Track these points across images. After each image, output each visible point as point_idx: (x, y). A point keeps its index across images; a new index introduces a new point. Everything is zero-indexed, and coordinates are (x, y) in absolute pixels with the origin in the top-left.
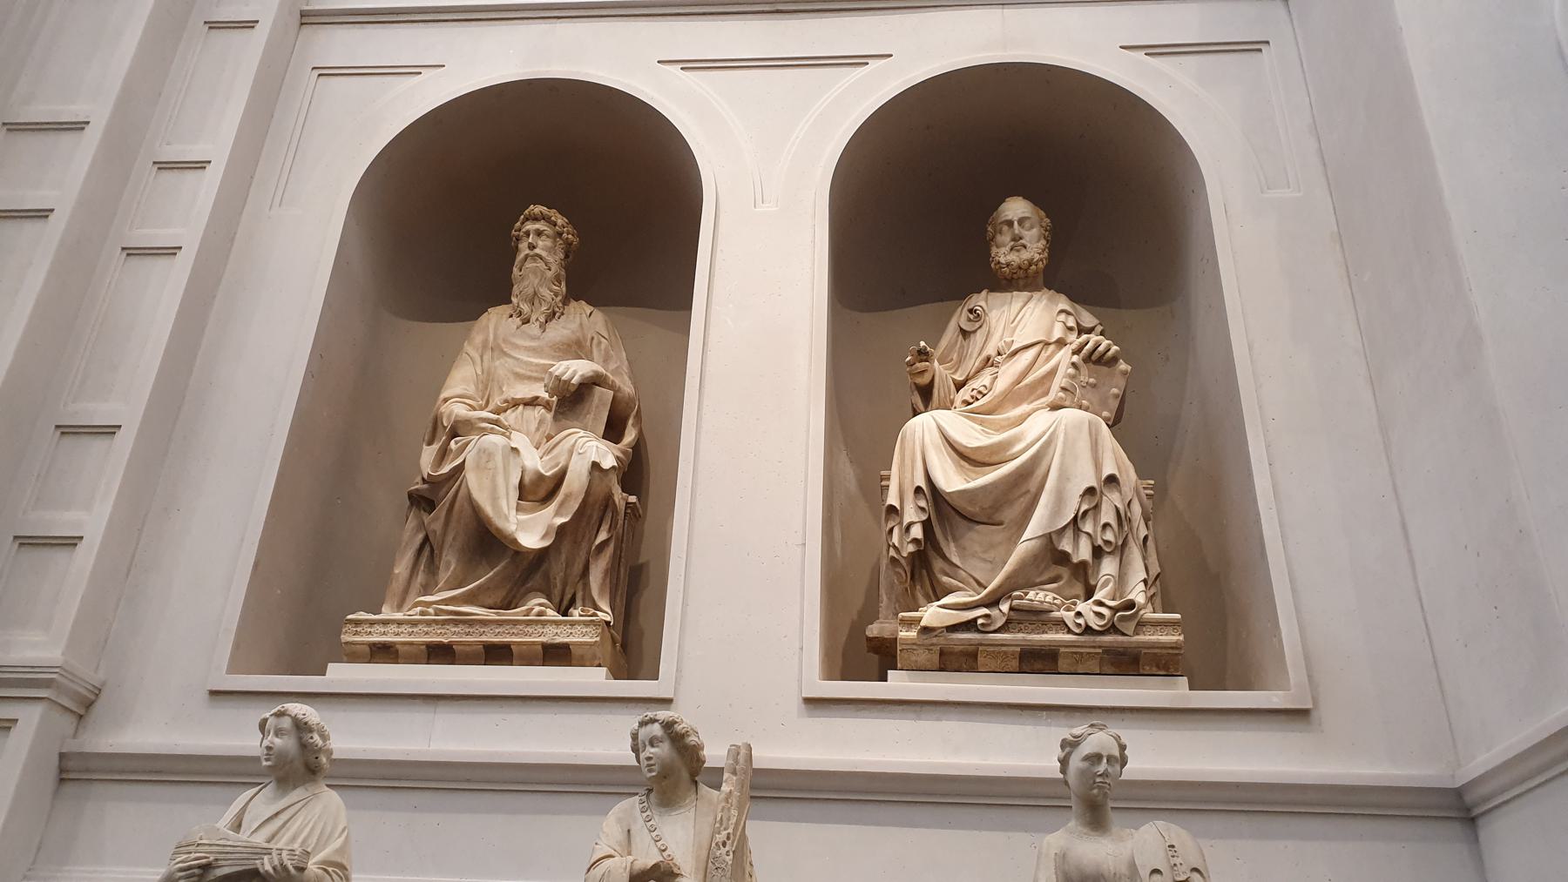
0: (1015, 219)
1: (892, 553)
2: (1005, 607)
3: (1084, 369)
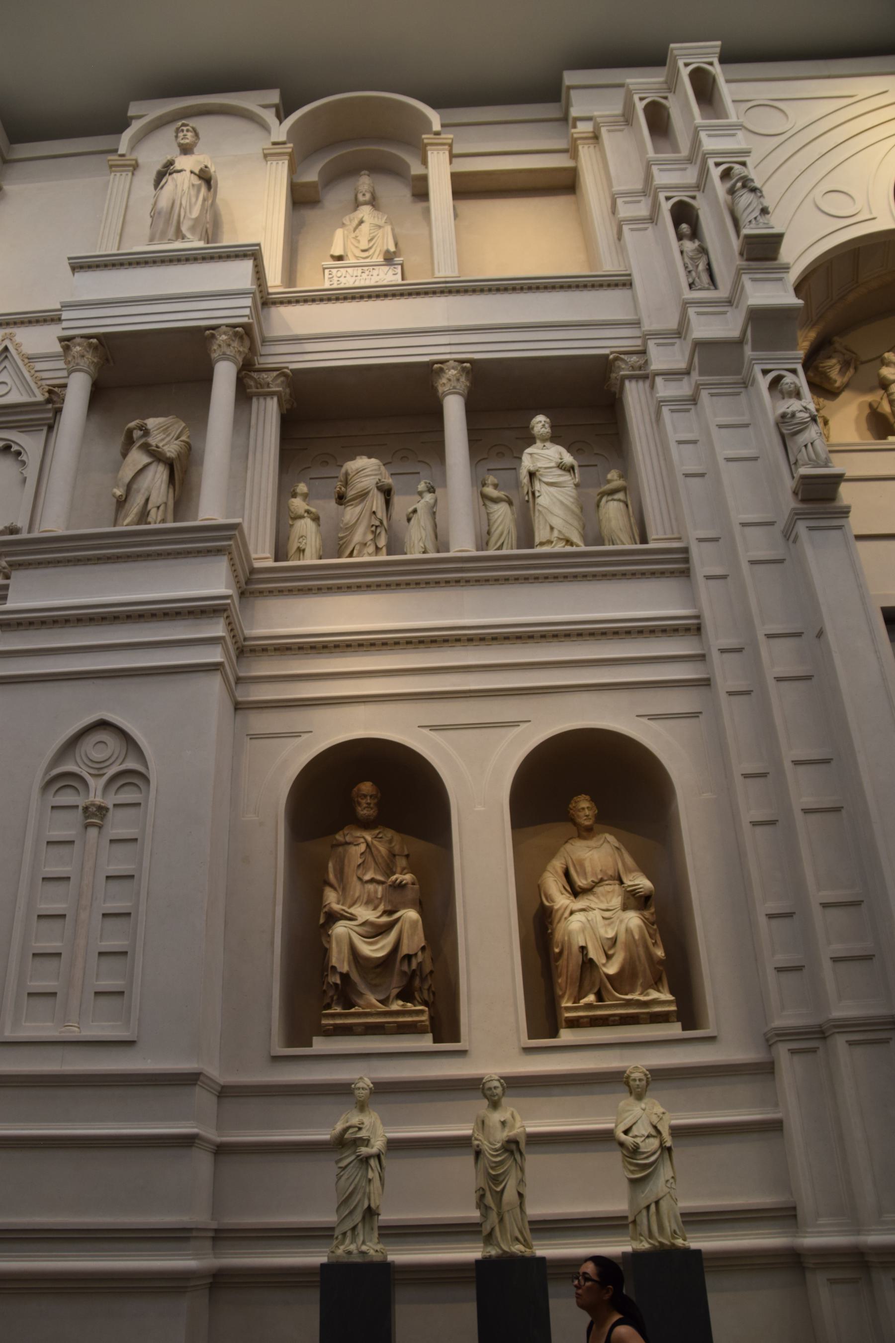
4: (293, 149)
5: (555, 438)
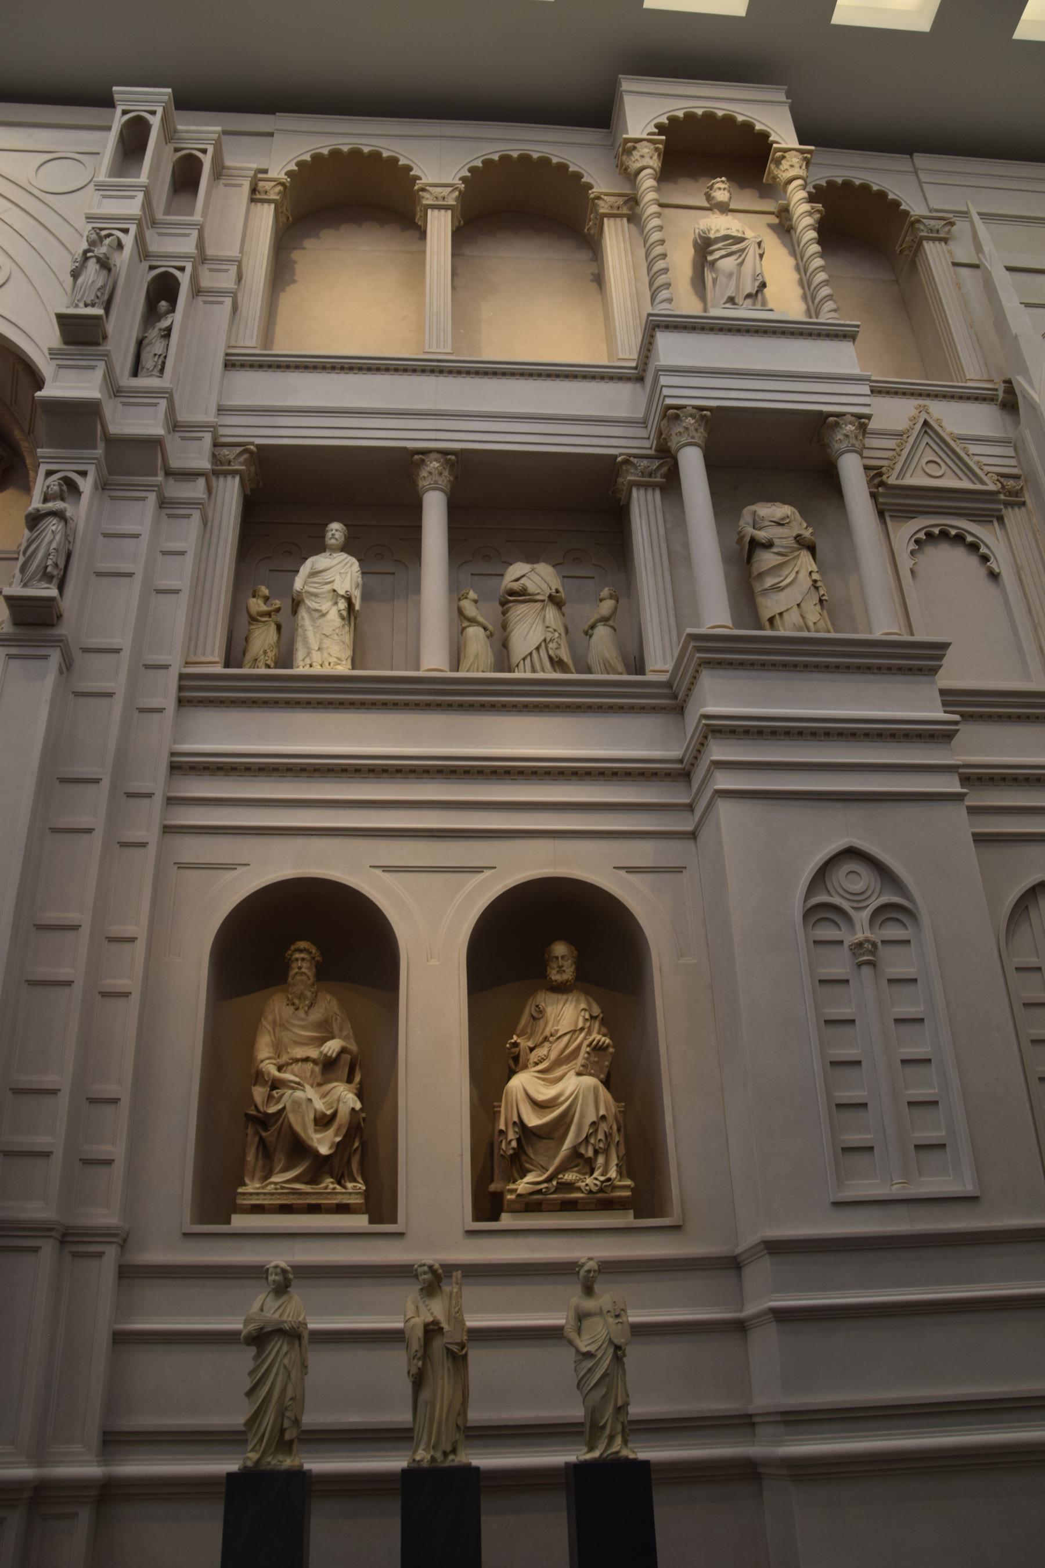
0: (560, 956)
1: (502, 1152)
2: (554, 1183)
3: (593, 1055)
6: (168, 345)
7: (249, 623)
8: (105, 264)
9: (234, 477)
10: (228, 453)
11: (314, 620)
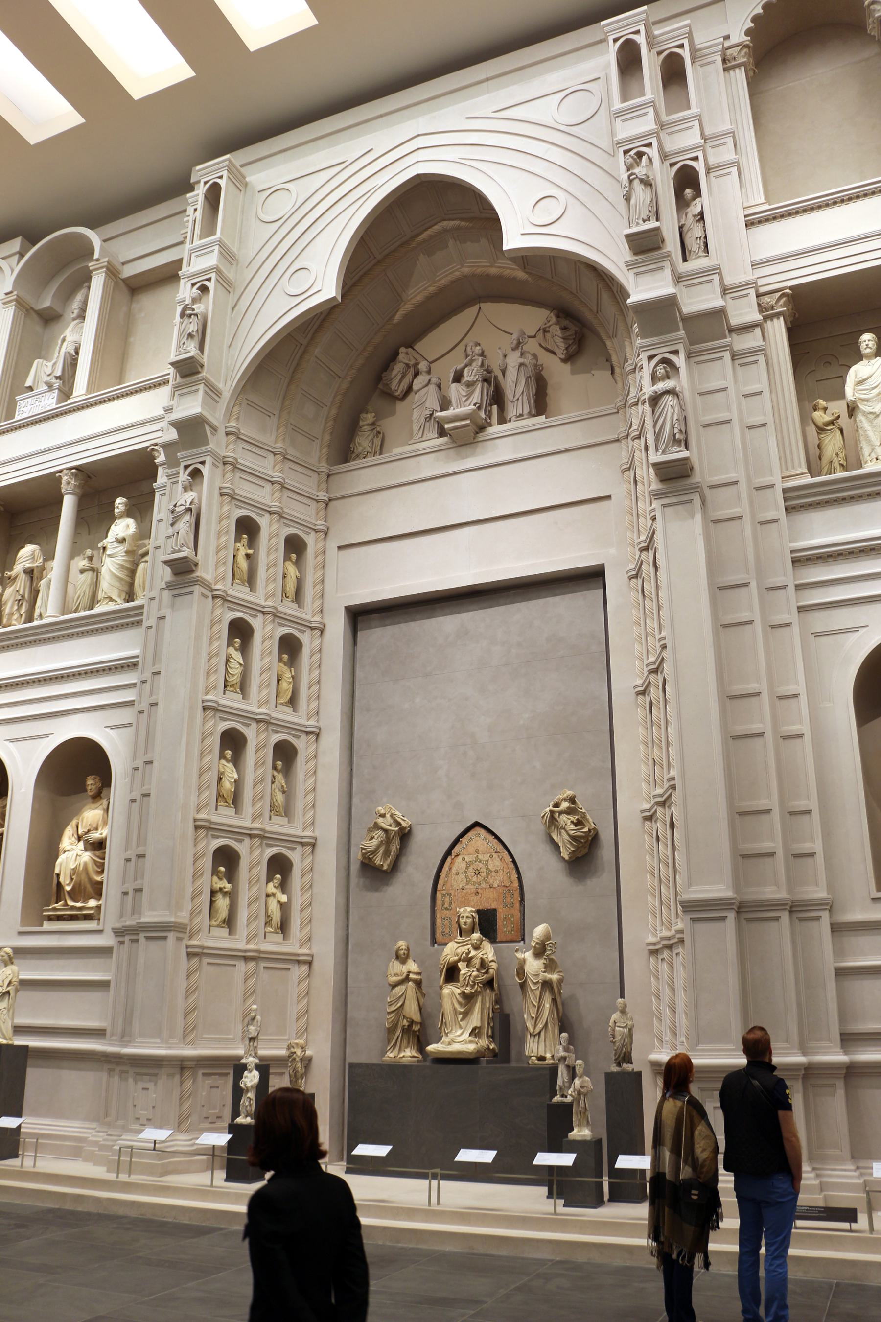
4: (17, 296)
5: (128, 513)
6: (704, 227)
7: (818, 432)
8: (647, 183)
9: (778, 318)
10: (769, 300)
11: (871, 421)
